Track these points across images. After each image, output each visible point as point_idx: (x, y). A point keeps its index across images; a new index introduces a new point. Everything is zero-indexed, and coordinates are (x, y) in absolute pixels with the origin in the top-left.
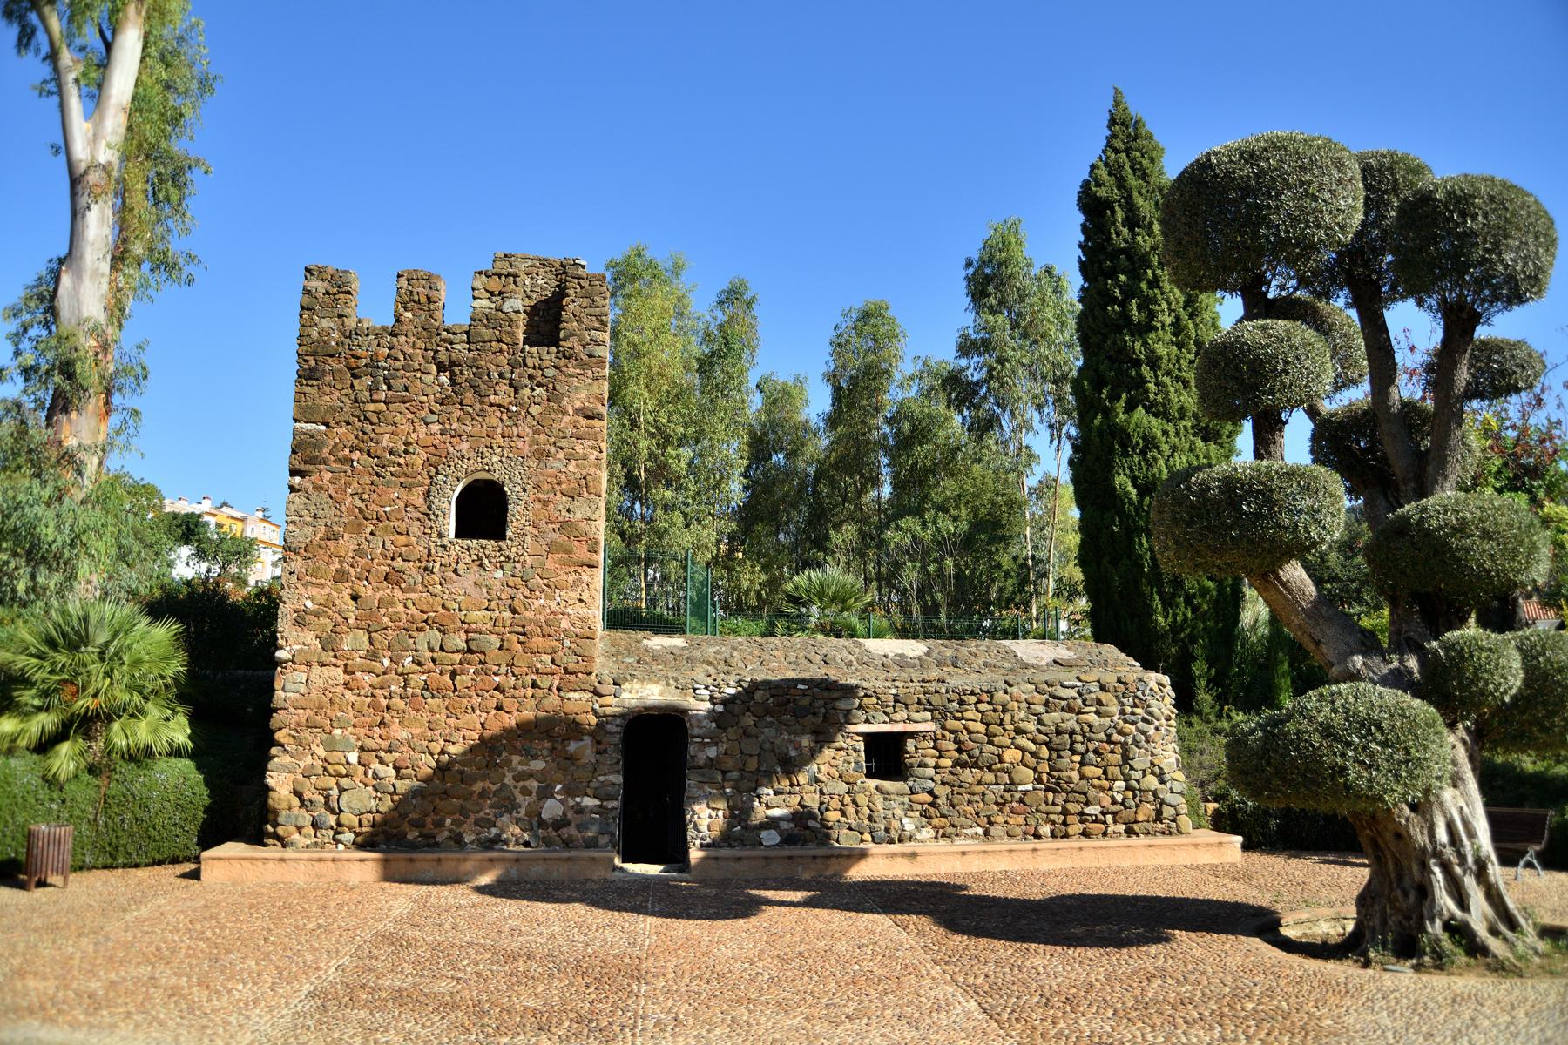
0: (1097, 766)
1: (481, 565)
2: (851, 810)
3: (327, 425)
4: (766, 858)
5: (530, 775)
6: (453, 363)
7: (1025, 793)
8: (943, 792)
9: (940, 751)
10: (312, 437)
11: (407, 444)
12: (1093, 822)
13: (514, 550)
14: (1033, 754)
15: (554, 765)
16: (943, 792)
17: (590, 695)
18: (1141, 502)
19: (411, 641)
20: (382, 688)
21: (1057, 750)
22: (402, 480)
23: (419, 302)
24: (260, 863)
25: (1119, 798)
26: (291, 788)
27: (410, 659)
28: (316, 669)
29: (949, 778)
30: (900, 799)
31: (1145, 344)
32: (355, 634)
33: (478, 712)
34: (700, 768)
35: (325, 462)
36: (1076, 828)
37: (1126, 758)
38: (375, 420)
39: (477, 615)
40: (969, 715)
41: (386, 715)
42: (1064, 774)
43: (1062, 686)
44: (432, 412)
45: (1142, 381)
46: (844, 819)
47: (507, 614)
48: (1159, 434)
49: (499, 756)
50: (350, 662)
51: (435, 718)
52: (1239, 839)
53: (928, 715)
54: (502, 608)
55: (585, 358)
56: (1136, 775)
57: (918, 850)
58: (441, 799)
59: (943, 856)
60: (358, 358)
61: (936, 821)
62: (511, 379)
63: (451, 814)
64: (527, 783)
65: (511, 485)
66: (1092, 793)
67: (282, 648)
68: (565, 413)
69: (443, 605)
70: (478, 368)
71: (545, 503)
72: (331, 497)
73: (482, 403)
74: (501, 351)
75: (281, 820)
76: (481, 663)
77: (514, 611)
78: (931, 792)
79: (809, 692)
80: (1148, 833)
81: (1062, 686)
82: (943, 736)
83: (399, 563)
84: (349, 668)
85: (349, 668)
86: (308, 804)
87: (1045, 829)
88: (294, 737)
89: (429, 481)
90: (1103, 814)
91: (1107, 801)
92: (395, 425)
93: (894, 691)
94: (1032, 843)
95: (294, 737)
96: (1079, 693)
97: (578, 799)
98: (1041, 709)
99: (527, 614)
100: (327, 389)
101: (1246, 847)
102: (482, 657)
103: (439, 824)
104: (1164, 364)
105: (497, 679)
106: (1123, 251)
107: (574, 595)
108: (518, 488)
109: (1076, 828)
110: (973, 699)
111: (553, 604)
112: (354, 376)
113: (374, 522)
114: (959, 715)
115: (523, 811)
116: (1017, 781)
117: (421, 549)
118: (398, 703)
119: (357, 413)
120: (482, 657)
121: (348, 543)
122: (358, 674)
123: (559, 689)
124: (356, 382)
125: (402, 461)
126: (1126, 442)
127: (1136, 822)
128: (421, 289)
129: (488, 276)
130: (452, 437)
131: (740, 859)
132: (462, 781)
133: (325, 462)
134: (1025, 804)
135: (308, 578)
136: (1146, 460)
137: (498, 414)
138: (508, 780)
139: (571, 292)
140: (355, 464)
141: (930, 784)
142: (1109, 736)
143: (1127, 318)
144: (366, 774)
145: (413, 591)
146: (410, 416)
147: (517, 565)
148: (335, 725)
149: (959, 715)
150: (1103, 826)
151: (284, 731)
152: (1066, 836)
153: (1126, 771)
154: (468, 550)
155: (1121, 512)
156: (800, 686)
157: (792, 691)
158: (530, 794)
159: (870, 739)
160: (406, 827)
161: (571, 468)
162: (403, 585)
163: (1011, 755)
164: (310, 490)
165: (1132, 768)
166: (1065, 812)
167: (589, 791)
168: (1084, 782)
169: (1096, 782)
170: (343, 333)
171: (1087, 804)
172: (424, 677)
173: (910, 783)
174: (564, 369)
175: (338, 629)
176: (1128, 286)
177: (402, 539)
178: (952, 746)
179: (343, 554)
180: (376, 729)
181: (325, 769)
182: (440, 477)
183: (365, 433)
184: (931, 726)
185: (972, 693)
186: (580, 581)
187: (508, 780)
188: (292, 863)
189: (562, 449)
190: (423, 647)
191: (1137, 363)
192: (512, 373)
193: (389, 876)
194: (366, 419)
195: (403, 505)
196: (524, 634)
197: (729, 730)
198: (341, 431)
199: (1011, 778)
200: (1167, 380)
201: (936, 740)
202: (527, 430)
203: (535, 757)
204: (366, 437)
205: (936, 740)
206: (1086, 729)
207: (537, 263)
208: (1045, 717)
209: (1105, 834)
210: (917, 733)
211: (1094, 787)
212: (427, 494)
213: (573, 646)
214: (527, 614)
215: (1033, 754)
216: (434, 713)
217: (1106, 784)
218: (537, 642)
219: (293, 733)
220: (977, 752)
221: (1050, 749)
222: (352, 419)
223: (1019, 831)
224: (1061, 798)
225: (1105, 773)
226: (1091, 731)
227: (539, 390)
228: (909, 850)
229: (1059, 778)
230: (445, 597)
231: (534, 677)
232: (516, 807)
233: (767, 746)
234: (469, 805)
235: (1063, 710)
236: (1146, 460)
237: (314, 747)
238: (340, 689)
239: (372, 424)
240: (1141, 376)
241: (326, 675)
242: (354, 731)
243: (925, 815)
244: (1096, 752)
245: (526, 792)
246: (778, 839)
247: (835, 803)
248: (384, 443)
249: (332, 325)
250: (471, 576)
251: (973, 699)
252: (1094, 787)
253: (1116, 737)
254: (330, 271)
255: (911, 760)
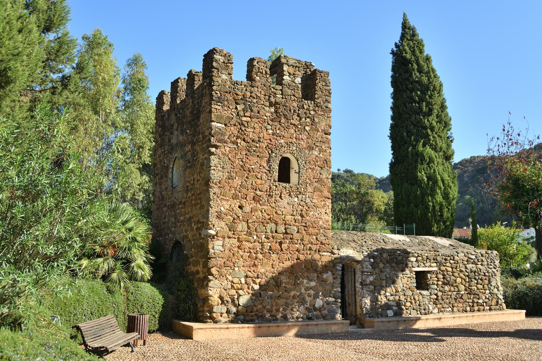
0: (481, 285)
1: (290, 195)
2: (413, 302)
3: (226, 125)
4: (398, 321)
5: (311, 288)
6: (276, 103)
7: (462, 295)
8: (440, 294)
9: (438, 279)
10: (220, 130)
11: (259, 137)
12: (480, 306)
13: (302, 189)
14: (464, 280)
15: (319, 284)
16: (440, 294)
17: (330, 254)
18: (428, 183)
19: (264, 228)
20: (253, 249)
21: (471, 278)
22: (258, 154)
23: (262, 73)
24: (218, 330)
25: (487, 296)
26: (218, 295)
27: (264, 236)
28: (227, 240)
29: (441, 289)
30: (427, 297)
31: (428, 121)
32: (242, 224)
33: (290, 261)
34: (367, 285)
35: (226, 142)
36: (476, 308)
37: (490, 282)
38: (246, 125)
39: (289, 217)
40: (448, 264)
41: (256, 261)
42: (473, 288)
43: (471, 254)
44: (269, 124)
45: (428, 135)
46: (412, 306)
47: (300, 218)
48: (434, 157)
49: (299, 280)
50: (240, 237)
51: (274, 263)
52: (524, 311)
53: (435, 264)
54: (297, 215)
55: (324, 108)
56: (492, 288)
57: (442, 317)
58: (278, 299)
59: (448, 319)
60: (238, 95)
61: (439, 306)
62: (298, 113)
63: (282, 306)
64: (309, 292)
65: (301, 161)
66: (481, 294)
67: (211, 229)
68: (318, 131)
69: (276, 212)
70: (286, 107)
71: (313, 169)
72: (229, 159)
73: (288, 122)
74: (294, 100)
75: (215, 310)
76: (291, 239)
77: (302, 216)
78: (436, 295)
79: (401, 254)
80: (495, 310)
81: (471, 254)
82: (440, 272)
83: (258, 193)
84: (240, 240)
85: (240, 240)
86: (226, 302)
87: (468, 309)
88: (218, 271)
89: (268, 156)
90: (483, 302)
91: (484, 298)
92: (255, 128)
93: (427, 255)
94: (465, 314)
95: (218, 271)
96: (476, 257)
97: (327, 299)
98: (466, 263)
99: (308, 218)
100: (226, 108)
101: (528, 315)
102: (292, 236)
103: (278, 310)
104: (436, 130)
105: (297, 246)
106: (416, 82)
107: (323, 210)
108: (303, 162)
109: (476, 308)
110: (449, 258)
111: (316, 214)
112: (237, 103)
113: (248, 172)
114: (445, 264)
115: (308, 304)
116: (460, 290)
117: (266, 187)
118: (260, 256)
119: (239, 121)
120: (292, 236)
121: (237, 182)
122: (244, 242)
123: (319, 251)
124: (238, 106)
125: (258, 145)
126: (423, 159)
127: (492, 305)
128: (262, 67)
129: (288, 66)
130: (277, 136)
131: (389, 322)
132: (286, 291)
133: (226, 142)
134: (462, 299)
135: (222, 197)
136: (430, 167)
137: (294, 128)
138: (303, 291)
139: (318, 78)
140: (239, 144)
141: (436, 291)
142: (485, 273)
143: (420, 108)
144: (248, 288)
145: (265, 205)
146: (260, 125)
147: (304, 196)
148: (236, 265)
149: (445, 264)
150: (483, 307)
151: (214, 268)
152: (474, 311)
153: (490, 286)
154: (285, 188)
155: (420, 186)
156: (398, 252)
157: (396, 254)
158: (311, 296)
159: (417, 273)
160: (265, 312)
161: (321, 155)
162: (261, 202)
163: (459, 280)
164: (220, 155)
165: (491, 286)
166: (473, 302)
167: (331, 295)
168: (478, 291)
169: (481, 291)
170: (231, 82)
171: (479, 299)
172: (269, 244)
173: (430, 291)
174: (317, 111)
175: (236, 221)
176: (420, 96)
177: (259, 181)
178: (442, 277)
179: (236, 186)
180: (252, 268)
181: (232, 286)
182: (274, 154)
183: (242, 131)
184: (435, 269)
185: (449, 256)
186: (325, 204)
187: (303, 291)
188: (231, 330)
189: (317, 146)
190: (269, 231)
191: (425, 128)
192: (299, 110)
193: (259, 335)
194: (243, 124)
195: (259, 165)
196: (306, 227)
197: (376, 269)
198: (232, 128)
199: (459, 289)
200: (436, 136)
201: (437, 274)
202: (305, 136)
203: (311, 281)
204: (243, 133)
205: (437, 274)
206: (479, 271)
207: (296, 61)
208: (468, 266)
209: (484, 310)
210: (431, 271)
211: (481, 292)
212: (268, 161)
213: (324, 232)
214: (308, 218)
215: (464, 280)
216: (274, 261)
217: (484, 291)
218: (311, 230)
219: (218, 269)
220: (449, 279)
221: (469, 278)
222: (237, 124)
223: (461, 309)
224: (472, 296)
225: (483, 287)
226: (480, 272)
227: (308, 120)
228: (439, 317)
229: (471, 289)
230: (277, 209)
231: (310, 245)
232: (306, 302)
233: (388, 276)
234: (289, 301)
235: (472, 263)
236: (430, 167)
237: (227, 276)
238: (236, 249)
239: (245, 126)
240: (427, 133)
241: (231, 242)
242: (244, 269)
243: (435, 303)
244: (481, 280)
245: (309, 295)
246: (392, 314)
247: (409, 299)
248: (251, 136)
249: (227, 78)
250: (286, 199)
251: (449, 258)
252: (481, 292)
253: (487, 274)
254: (225, 52)
255: (430, 282)
